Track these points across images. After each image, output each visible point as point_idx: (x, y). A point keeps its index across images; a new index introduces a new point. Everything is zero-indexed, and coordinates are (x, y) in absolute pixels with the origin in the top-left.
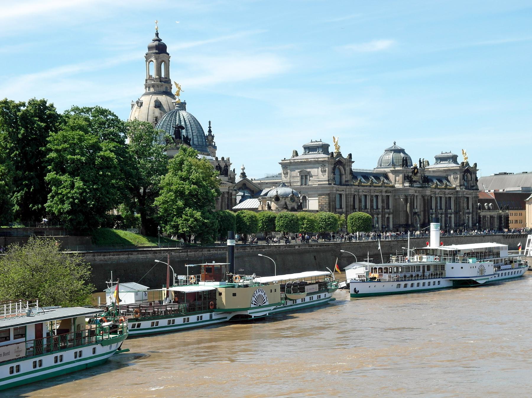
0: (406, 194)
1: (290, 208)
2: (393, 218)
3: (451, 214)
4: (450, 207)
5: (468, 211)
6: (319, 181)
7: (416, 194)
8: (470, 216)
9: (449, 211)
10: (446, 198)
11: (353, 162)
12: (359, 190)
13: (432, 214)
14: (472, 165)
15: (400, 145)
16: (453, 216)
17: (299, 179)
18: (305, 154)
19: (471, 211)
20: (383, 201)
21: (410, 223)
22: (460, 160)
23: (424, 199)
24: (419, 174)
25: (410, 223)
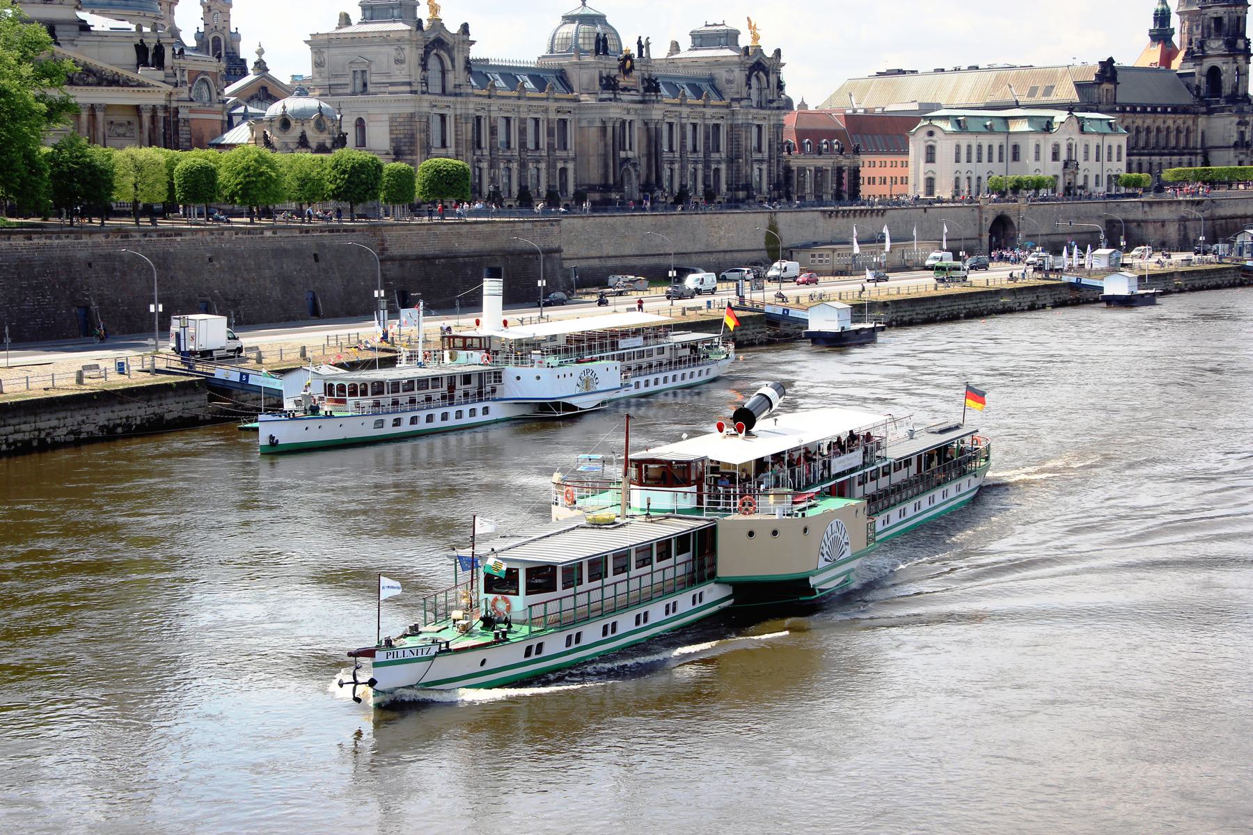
0: (604, 116)
1: (313, 145)
2: (575, 170)
3: (719, 162)
4: (718, 147)
5: (759, 156)
6: (392, 84)
7: (628, 118)
8: (764, 166)
9: (715, 156)
10: (706, 126)
11: (473, 42)
12: (489, 106)
13: (672, 163)
14: (769, 53)
15: (596, 4)
16: (723, 167)
17: (348, 80)
18: (365, 21)
19: (766, 155)
20: (550, 133)
21: (611, 181)
22: (744, 40)
23: (648, 129)
24: (634, 73)
25: (611, 181)
